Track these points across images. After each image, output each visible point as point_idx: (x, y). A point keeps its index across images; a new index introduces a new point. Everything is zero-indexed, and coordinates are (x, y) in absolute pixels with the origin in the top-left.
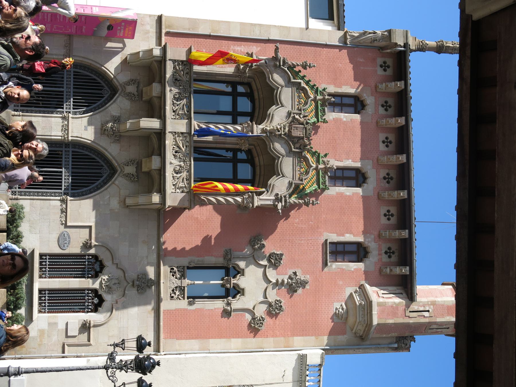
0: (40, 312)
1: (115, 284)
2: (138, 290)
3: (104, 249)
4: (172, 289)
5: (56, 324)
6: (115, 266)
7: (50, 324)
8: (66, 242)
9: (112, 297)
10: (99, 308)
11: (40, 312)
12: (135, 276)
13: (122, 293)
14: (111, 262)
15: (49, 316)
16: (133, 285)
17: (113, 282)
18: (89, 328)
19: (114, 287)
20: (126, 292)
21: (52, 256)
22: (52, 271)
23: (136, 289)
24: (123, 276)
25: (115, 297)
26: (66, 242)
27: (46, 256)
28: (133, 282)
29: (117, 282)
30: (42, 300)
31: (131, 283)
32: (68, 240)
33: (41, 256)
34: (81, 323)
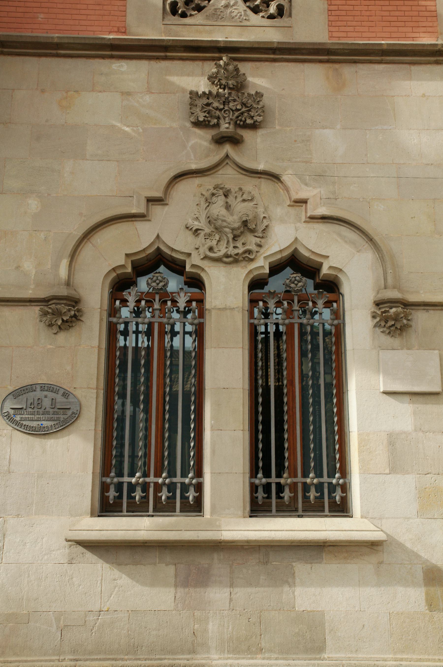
0: (342, 508)
1: (228, 207)
2: (254, 126)
3: (87, 251)
4: (249, 12)
5: (392, 440)
6: (157, 210)
7: (395, 467)
8: (47, 403)
9: (282, 221)
10: (325, 270)
11: (342, 508)
12: (202, 139)
13: (266, 186)
14: (140, 225)
15: (363, 471)
16: (235, 141)
17: (224, 212)
18: (406, 305)
19: (241, 209)
20: (261, 167)
21: (111, 460)
22: (172, 463)
23: (247, 134)
24: (197, 181)
25: (278, 211)
26: (47, 403)
27: (104, 488)
28: (220, 140)
29: (220, 200)
30: (294, 499)
31: (228, 148)
32: (38, 394)
33: (106, 507)
34: (386, 340)
